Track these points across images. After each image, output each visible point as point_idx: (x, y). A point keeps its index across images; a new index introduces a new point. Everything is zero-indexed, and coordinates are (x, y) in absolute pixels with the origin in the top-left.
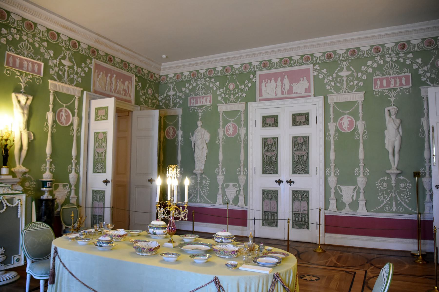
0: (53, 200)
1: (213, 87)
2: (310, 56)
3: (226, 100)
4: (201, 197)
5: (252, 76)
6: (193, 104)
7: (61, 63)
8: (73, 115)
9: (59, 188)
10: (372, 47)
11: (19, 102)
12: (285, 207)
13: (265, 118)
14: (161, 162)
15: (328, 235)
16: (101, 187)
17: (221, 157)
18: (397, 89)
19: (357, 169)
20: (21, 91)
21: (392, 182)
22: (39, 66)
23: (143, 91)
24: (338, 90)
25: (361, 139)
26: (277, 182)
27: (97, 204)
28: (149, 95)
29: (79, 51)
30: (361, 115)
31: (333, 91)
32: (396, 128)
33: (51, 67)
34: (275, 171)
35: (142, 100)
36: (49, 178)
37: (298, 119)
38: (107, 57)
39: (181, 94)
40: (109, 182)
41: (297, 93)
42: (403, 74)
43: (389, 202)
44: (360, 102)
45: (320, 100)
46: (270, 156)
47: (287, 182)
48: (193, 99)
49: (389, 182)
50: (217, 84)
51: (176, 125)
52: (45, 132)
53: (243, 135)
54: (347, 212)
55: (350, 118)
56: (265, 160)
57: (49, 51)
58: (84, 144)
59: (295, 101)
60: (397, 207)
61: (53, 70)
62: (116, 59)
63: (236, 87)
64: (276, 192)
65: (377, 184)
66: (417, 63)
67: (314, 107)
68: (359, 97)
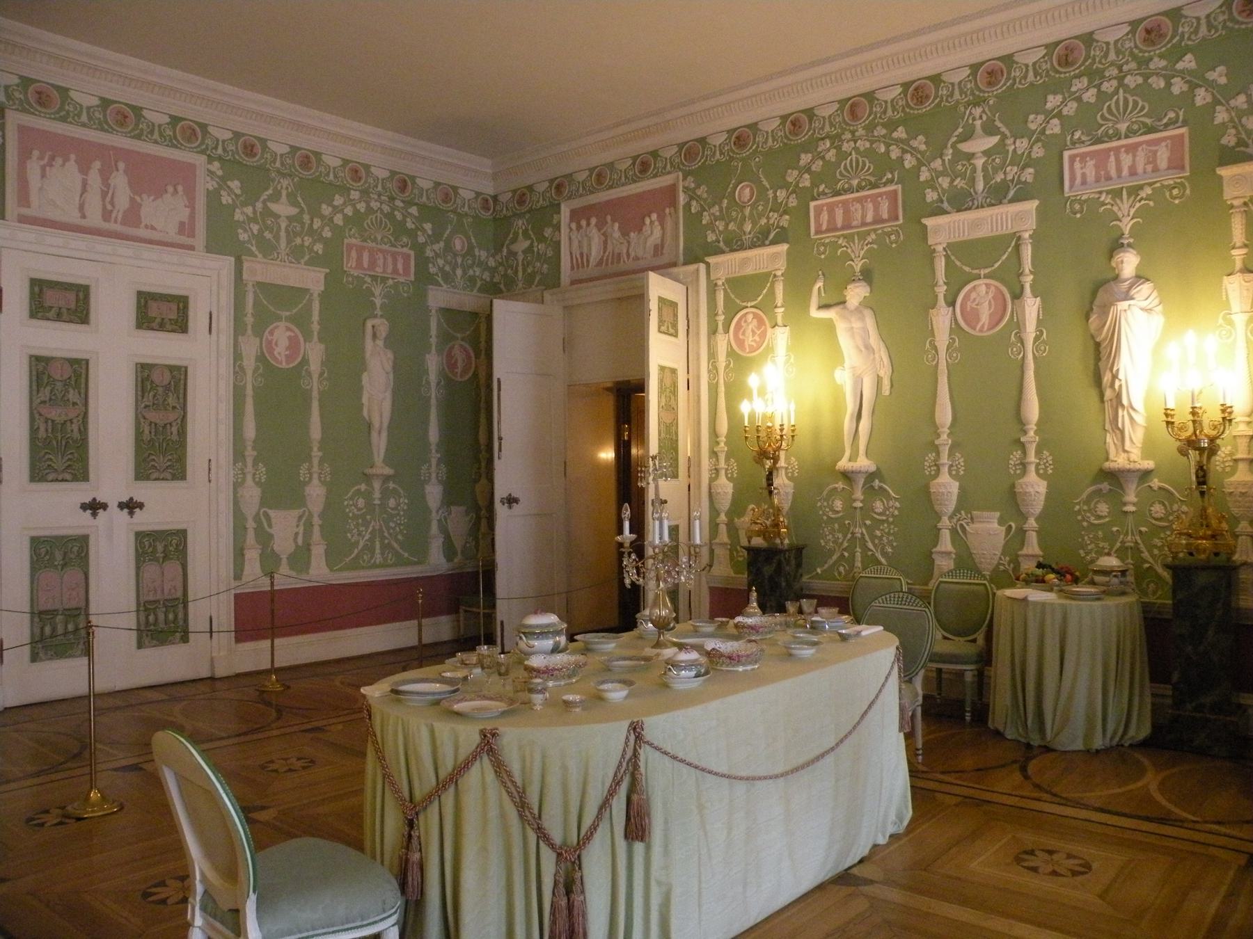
2: (198, 130)
10: (346, 162)
12: (113, 584)
15: (240, 645)
19: (306, 465)
24: (268, 249)
26: (84, 507)
30: (316, 327)
31: (254, 249)
34: (78, 470)
37: (154, 309)
41: (153, 228)
42: (399, 250)
47: (121, 506)
49: (368, 495)
54: (286, 579)
60: (382, 554)
64: (83, 541)
66: (424, 231)
68: (313, 279)
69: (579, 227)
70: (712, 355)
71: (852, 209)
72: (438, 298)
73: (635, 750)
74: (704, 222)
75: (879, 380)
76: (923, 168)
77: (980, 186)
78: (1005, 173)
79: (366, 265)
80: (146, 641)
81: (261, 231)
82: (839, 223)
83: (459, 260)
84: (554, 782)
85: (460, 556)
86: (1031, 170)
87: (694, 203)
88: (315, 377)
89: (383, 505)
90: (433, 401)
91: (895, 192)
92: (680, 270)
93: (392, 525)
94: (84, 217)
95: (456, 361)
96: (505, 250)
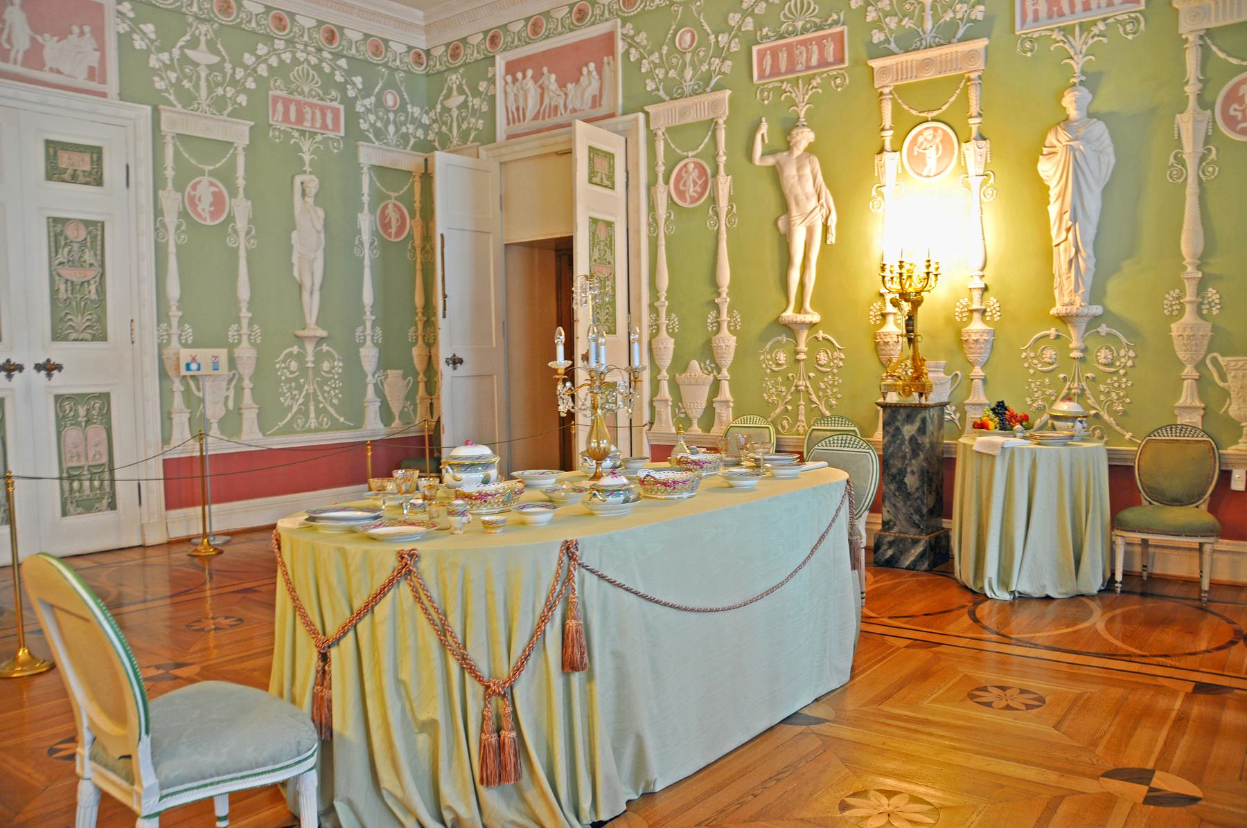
18: (316, 134)
19: (235, 327)
25: (242, 248)
30: (241, 182)
37: (64, 160)
42: (328, 103)
47: (38, 367)
49: (300, 358)
54: (217, 445)
55: (216, 186)
60: (317, 417)
66: (354, 84)
68: (239, 133)
69: (515, 80)
70: (652, 207)
71: (797, 52)
72: (368, 155)
73: (569, 570)
74: (643, 70)
75: (826, 228)
76: (870, 8)
77: (929, 25)
78: (954, 12)
79: (293, 118)
81: (179, 80)
82: (783, 67)
83: (391, 116)
84: (476, 608)
85: (397, 421)
86: (982, 8)
87: (633, 51)
88: (242, 234)
89: (317, 369)
90: (367, 262)
91: (842, 33)
92: (621, 120)
93: (327, 388)
95: (390, 222)
96: (439, 107)
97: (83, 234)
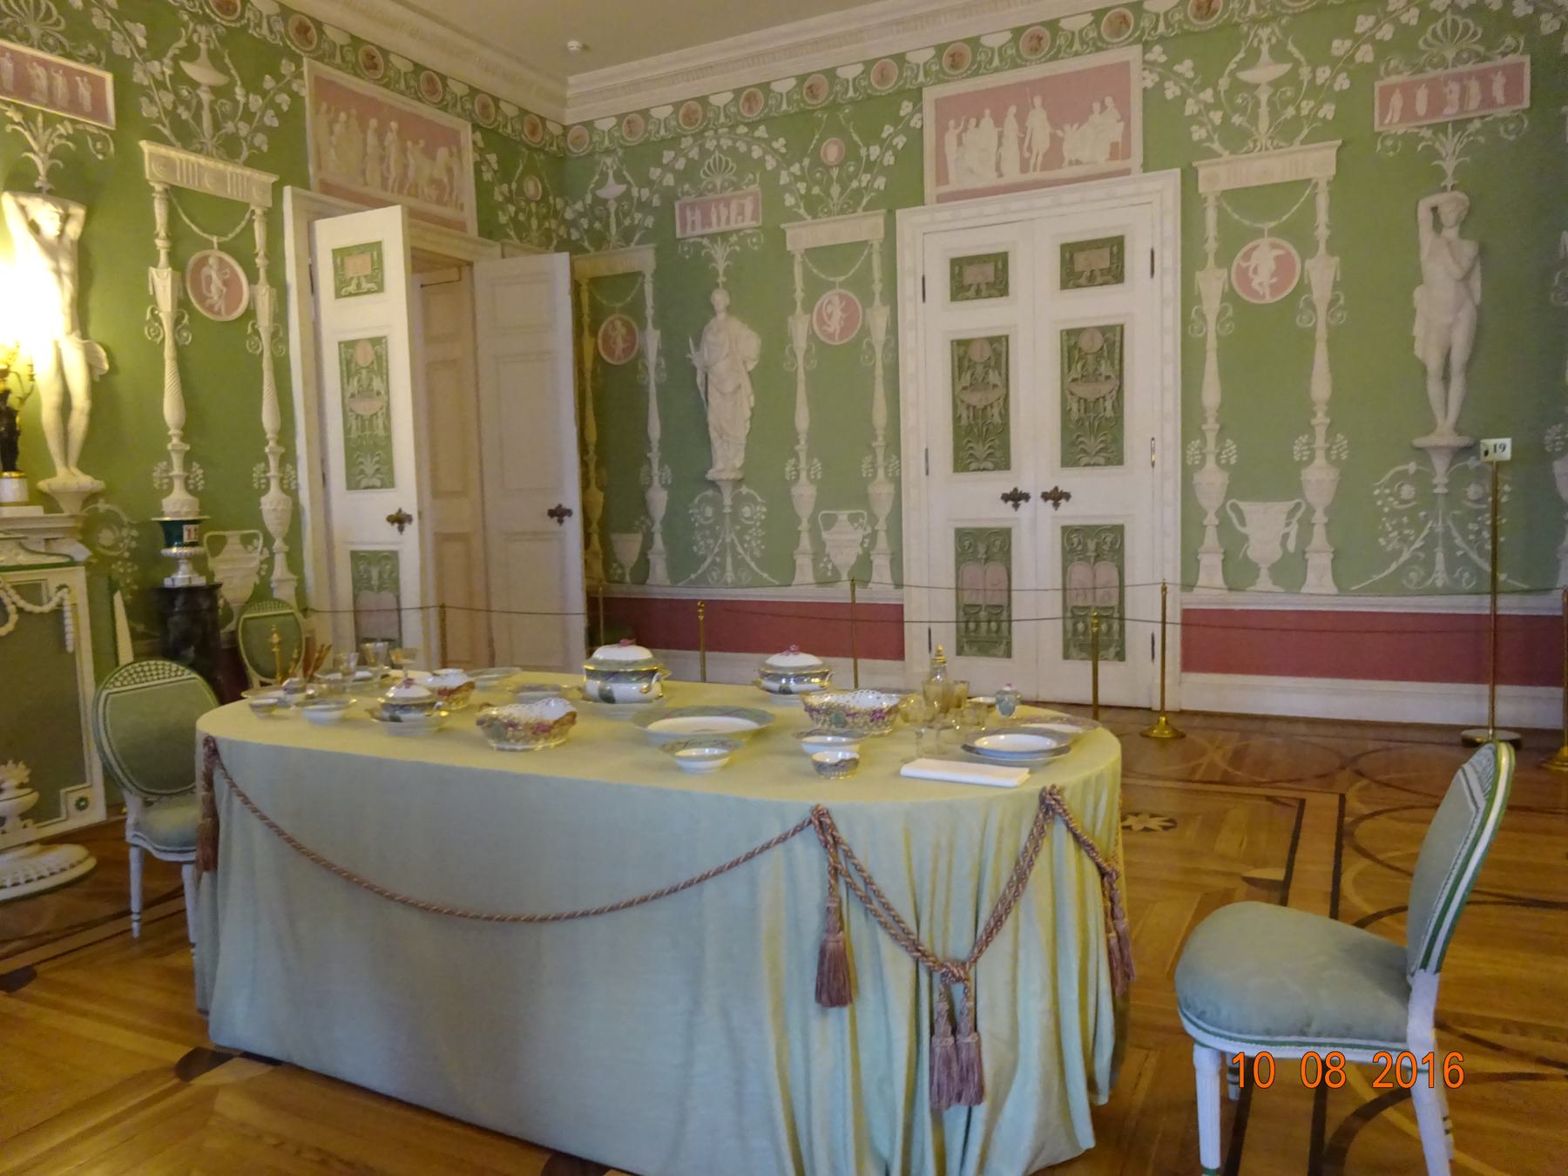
0: (212, 590)
1: (762, 160)
3: (814, 206)
4: (739, 564)
5: (906, 107)
6: (690, 227)
7: (179, 77)
8: (253, 279)
9: (227, 548)
11: (34, 227)
13: (959, 266)
14: (592, 448)
16: (382, 537)
17: (802, 420)
18: (1470, 120)
19: (1304, 439)
20: (37, 184)
21: (1435, 481)
22: (97, 84)
23: (505, 187)
24: (1237, 140)
26: (1006, 498)
27: (368, 599)
28: (528, 201)
29: (248, 25)
30: (1322, 232)
31: (1216, 146)
32: (1458, 274)
33: (143, 90)
34: (1001, 460)
35: (503, 219)
36: (187, 514)
37: (1081, 262)
38: (356, 51)
39: (645, 192)
40: (409, 519)
41: (1078, 162)
43: (1422, 555)
44: (1323, 185)
45: (1167, 183)
46: (980, 406)
47: (1045, 496)
48: (693, 206)
49: (1422, 480)
50: (779, 144)
51: (635, 310)
52: (152, 343)
53: (879, 335)
54: (1264, 596)
56: (964, 422)
57: (128, 24)
58: (305, 384)
59: (1069, 195)
60: (1450, 570)
61: (152, 101)
62: (392, 58)
63: (851, 153)
64: (1005, 534)
65: (1377, 492)
67: (1145, 211)
68: (1316, 162)
80: (1073, 651)
94: (1001, 175)
97: (1099, 342)
